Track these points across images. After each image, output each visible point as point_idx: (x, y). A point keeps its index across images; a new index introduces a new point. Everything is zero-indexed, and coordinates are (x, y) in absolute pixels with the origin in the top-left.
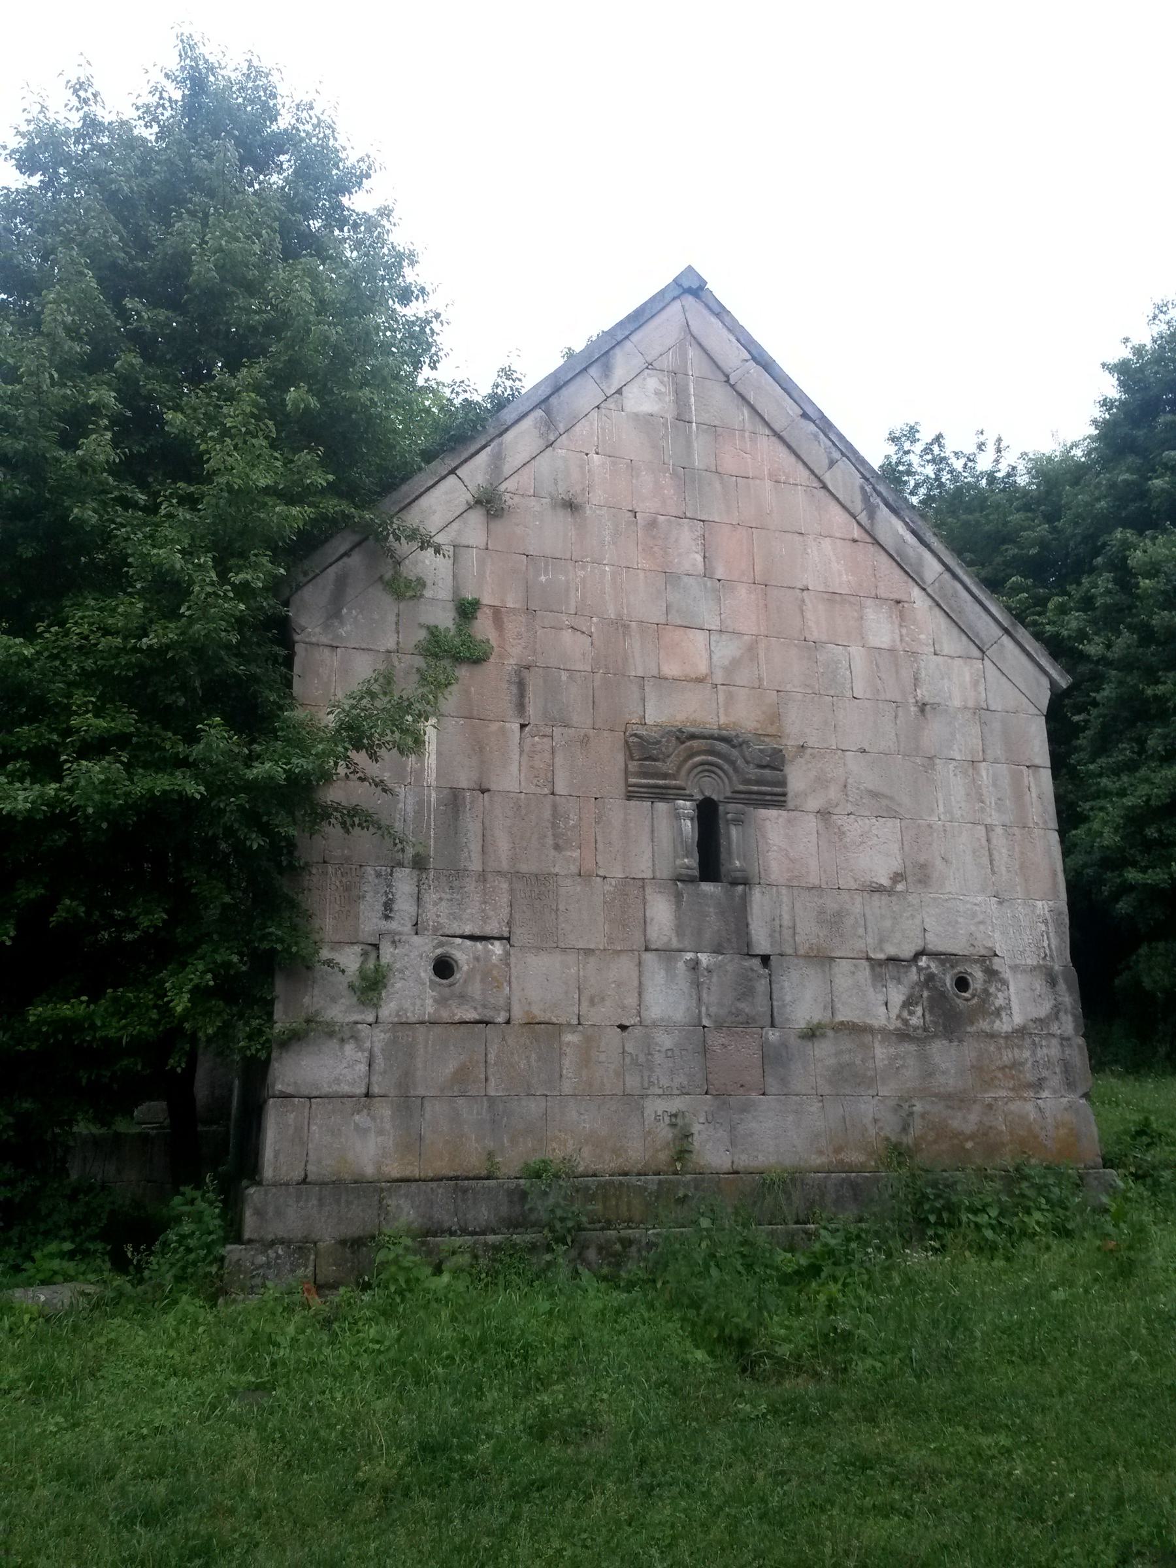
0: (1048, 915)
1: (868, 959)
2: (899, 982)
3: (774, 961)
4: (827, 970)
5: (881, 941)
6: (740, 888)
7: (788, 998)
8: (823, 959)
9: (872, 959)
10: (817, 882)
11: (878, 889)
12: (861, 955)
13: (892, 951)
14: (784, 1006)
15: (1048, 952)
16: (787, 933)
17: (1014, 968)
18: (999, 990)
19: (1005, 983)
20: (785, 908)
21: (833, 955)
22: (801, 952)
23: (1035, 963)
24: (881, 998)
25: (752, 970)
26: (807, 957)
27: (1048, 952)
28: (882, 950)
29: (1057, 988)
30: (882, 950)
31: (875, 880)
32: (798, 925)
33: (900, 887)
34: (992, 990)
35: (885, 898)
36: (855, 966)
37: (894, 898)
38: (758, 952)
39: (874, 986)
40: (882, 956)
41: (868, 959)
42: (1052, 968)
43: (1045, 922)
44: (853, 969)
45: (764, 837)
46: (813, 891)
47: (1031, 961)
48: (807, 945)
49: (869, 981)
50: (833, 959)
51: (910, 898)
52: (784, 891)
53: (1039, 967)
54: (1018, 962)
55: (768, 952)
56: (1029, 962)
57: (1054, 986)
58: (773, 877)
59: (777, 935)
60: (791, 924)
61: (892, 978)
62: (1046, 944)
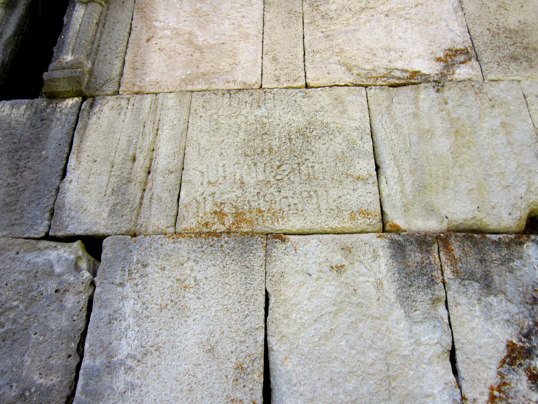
1: (385, 227)
2: (487, 285)
3: (107, 252)
4: (257, 262)
5: (421, 188)
6: (70, 102)
7: (125, 348)
8: (246, 235)
9: (397, 230)
10: (254, 79)
11: (413, 80)
12: (362, 223)
13: (459, 210)
14: (110, 367)
16: (161, 186)
20: (165, 133)
21: (279, 226)
22: (190, 222)
24: (431, 339)
25: (50, 273)
26: (206, 235)
28: (431, 210)
30: (431, 210)
31: (400, 65)
32: (192, 162)
33: (462, 72)
35: (427, 95)
36: (347, 250)
37: (451, 93)
38: (74, 229)
39: (405, 300)
40: (431, 225)
41: (385, 227)
44: (338, 258)
45: (145, 18)
46: (241, 95)
48: (209, 207)
49: (390, 290)
50: (281, 237)
51: (493, 90)
52: (171, 101)
55: (98, 227)
58: (153, 77)
59: (135, 190)
60: (175, 164)
61: (465, 277)
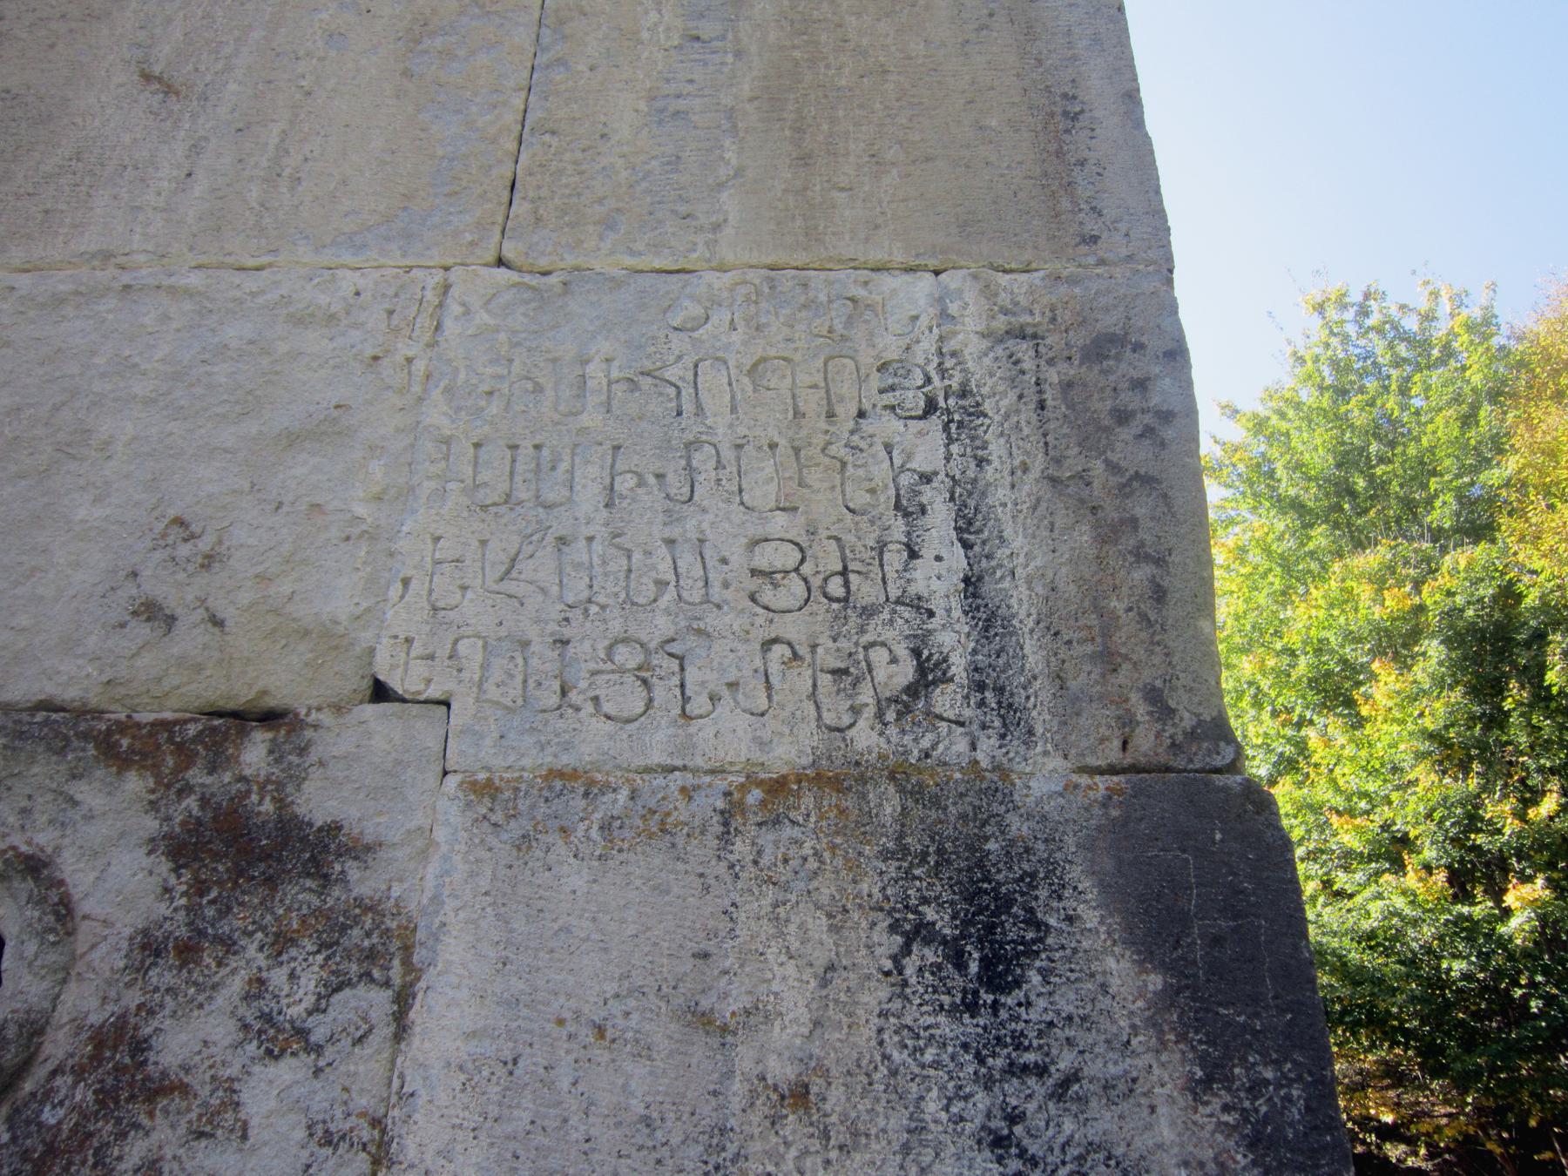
0: (980, 366)
15: (954, 641)
17: (528, 808)
18: (277, 1037)
19: (380, 953)
23: (789, 751)
27: (954, 641)
29: (1039, 998)
34: (175, 1046)
42: (994, 788)
43: (954, 412)
47: (756, 728)
53: (836, 779)
54: (591, 742)
56: (733, 739)
57: (999, 974)
62: (939, 574)
